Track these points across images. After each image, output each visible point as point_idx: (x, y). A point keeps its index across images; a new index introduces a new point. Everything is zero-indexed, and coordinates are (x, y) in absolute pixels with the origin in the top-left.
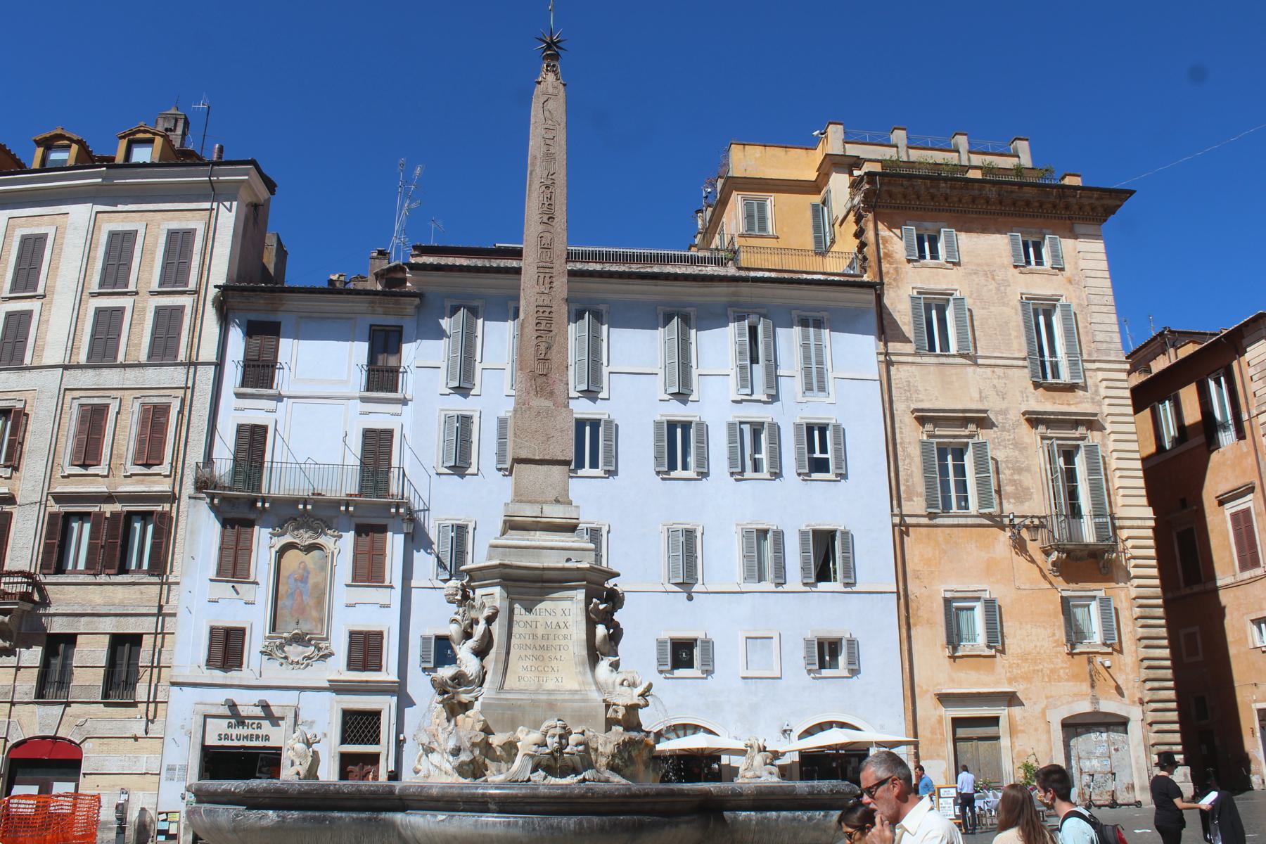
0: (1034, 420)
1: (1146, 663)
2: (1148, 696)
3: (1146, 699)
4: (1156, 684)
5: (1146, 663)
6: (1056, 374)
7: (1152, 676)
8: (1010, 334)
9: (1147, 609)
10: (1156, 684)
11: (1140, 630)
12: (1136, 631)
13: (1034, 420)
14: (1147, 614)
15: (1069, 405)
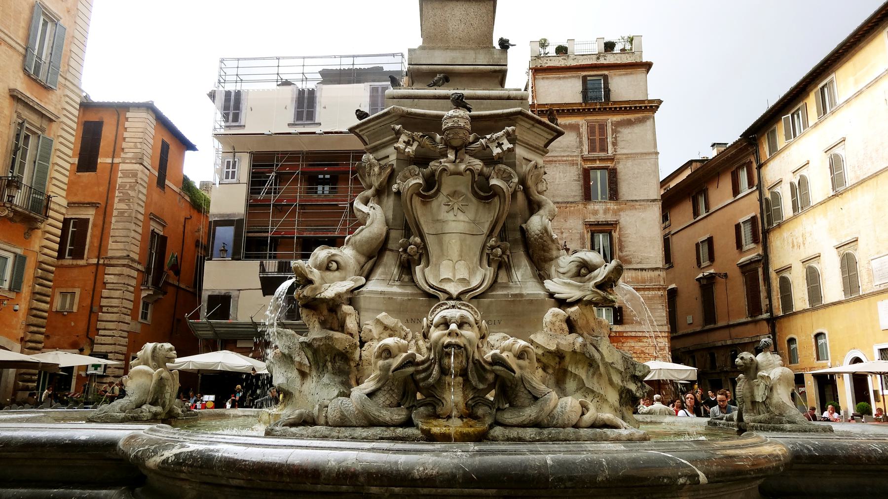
0: (15, 97)
1: (35, 312)
2: (29, 337)
3: (27, 339)
4: (35, 329)
5: (35, 312)
6: (37, 71)
7: (35, 322)
8: (20, 23)
9: (45, 272)
10: (35, 329)
11: (37, 286)
12: (34, 287)
13: (15, 97)
14: (44, 276)
15: (41, 101)
